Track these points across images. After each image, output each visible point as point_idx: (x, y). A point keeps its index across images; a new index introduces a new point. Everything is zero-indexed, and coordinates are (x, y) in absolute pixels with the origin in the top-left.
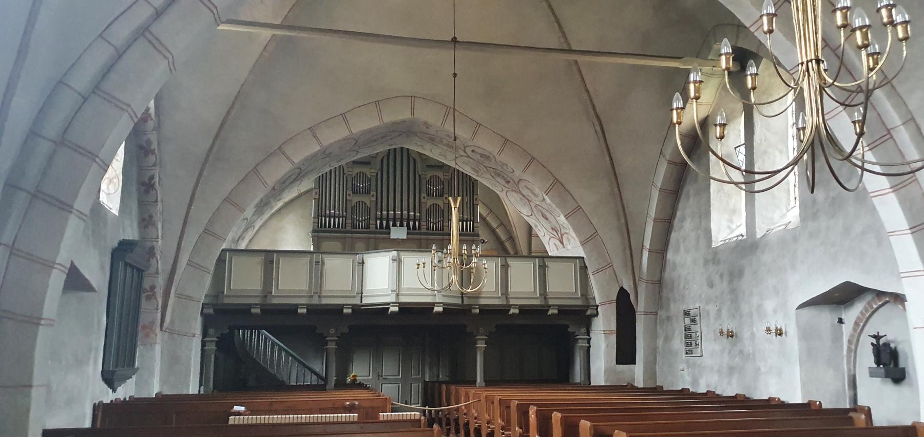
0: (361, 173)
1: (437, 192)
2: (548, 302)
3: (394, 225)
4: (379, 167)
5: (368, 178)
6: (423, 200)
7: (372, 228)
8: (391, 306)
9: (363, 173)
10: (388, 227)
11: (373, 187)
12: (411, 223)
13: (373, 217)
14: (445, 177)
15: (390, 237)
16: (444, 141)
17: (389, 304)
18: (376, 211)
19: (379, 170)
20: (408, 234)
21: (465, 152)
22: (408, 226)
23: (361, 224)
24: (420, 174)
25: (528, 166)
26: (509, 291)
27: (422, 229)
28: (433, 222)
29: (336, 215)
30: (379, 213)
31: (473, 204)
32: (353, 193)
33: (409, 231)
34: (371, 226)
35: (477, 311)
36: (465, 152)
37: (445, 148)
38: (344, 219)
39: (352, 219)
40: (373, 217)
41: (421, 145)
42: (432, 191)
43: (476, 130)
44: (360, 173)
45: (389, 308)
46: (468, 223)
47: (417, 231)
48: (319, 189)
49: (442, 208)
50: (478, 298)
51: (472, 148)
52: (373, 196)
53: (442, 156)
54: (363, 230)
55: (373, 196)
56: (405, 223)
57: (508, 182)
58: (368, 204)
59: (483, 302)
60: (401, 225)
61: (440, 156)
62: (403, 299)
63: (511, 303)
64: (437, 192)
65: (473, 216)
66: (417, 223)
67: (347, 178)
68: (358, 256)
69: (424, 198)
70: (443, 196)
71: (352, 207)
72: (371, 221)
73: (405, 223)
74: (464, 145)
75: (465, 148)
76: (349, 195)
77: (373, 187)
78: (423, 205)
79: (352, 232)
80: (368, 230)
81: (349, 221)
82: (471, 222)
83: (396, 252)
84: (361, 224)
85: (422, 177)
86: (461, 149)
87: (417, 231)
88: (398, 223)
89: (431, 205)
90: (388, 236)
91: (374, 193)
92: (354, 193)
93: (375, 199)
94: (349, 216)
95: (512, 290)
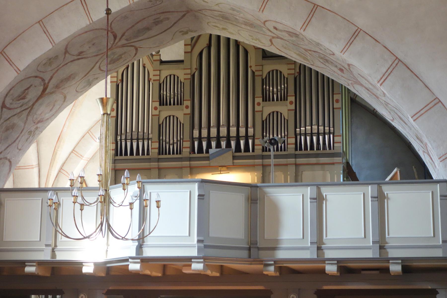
0: (172, 77)
2: (324, 254)
4: (195, 65)
6: (257, 108)
8: (131, 262)
9: (174, 76)
12: (242, 142)
17: (127, 260)
18: (193, 127)
19: (196, 69)
20: (234, 158)
24: (254, 71)
25: (350, 43)
26: (387, 236)
31: (333, 108)
35: (272, 268)
40: (187, 136)
45: (128, 265)
47: (251, 153)
49: (286, 118)
50: (274, 249)
52: (187, 107)
55: (187, 107)
56: (233, 143)
57: (341, 70)
58: (181, 119)
59: (281, 255)
62: (148, 253)
63: (390, 256)
66: (250, 141)
70: (287, 100)
73: (233, 143)
77: (187, 95)
78: (258, 116)
82: (331, 135)
85: (256, 73)
87: (243, 154)
88: (223, 144)
91: (188, 103)
95: (391, 236)
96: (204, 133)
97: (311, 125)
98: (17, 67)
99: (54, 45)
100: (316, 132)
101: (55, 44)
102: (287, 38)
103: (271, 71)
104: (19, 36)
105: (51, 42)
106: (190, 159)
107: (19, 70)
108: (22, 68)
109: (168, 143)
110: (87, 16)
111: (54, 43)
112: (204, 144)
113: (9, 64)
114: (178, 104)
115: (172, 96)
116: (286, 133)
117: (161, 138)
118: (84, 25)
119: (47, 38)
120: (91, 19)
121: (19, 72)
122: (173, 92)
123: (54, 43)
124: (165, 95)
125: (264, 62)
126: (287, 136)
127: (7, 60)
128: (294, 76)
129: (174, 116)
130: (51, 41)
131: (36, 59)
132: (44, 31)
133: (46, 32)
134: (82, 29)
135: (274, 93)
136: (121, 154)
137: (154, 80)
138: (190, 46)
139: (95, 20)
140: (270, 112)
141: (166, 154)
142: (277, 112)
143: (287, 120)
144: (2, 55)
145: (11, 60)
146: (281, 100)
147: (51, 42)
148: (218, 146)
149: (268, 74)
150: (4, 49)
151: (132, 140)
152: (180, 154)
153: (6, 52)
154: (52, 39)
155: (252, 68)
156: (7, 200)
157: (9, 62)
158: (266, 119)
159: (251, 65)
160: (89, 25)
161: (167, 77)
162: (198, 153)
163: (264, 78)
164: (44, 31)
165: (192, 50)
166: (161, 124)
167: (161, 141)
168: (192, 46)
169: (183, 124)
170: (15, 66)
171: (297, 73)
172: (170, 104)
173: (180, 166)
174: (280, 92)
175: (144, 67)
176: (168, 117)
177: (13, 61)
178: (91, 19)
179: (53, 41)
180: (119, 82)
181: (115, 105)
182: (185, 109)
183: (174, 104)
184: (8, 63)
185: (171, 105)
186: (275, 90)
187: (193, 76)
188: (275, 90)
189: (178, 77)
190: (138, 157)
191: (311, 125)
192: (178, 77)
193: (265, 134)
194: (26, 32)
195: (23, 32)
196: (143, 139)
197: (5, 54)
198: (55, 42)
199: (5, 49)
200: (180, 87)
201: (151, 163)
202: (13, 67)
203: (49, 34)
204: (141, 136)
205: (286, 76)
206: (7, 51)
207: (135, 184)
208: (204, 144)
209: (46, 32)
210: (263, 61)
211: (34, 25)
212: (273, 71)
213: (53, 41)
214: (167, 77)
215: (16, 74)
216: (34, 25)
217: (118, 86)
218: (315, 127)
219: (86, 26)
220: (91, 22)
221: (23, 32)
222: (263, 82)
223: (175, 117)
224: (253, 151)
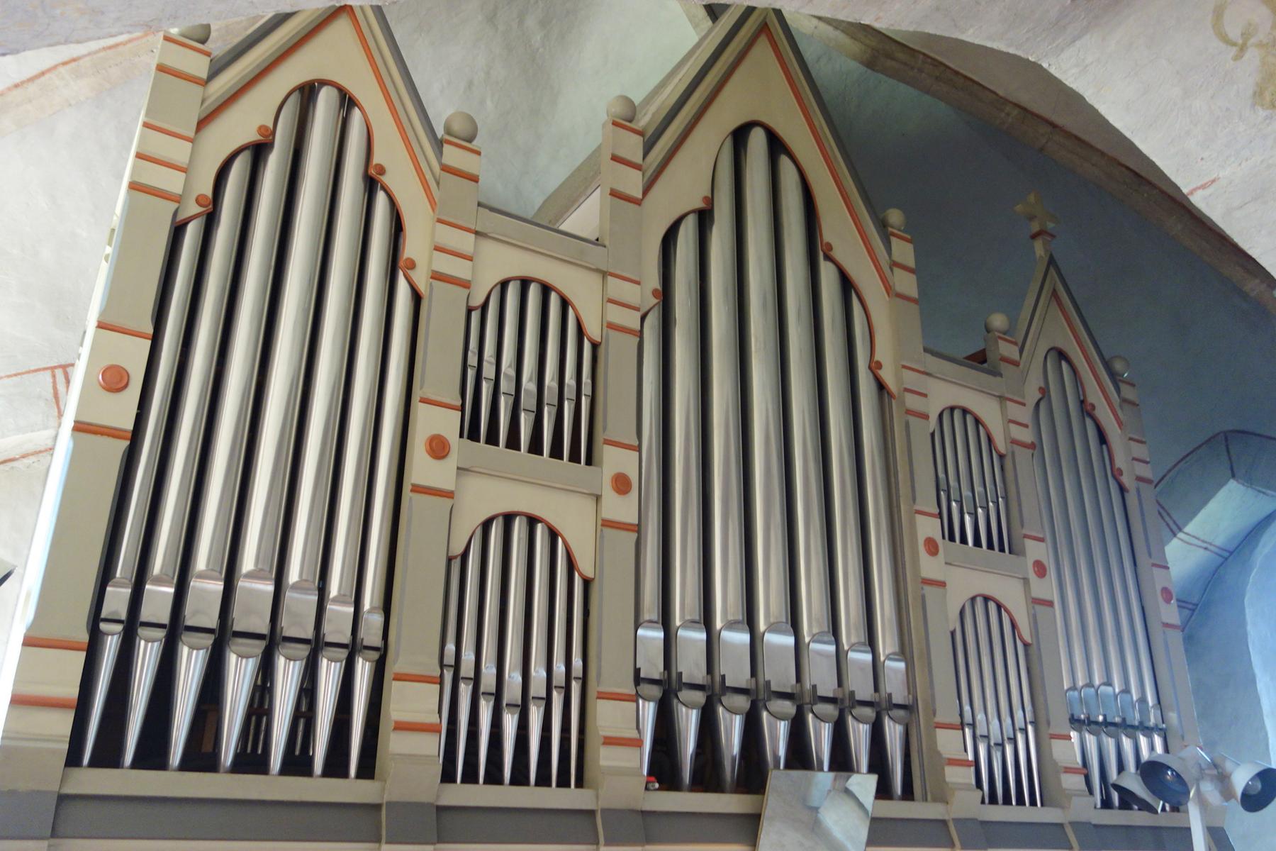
0: (533, 294)
9: (546, 290)
11: (616, 420)
23: (510, 723)
29: (288, 627)
38: (363, 671)
52: (621, 483)
84: (510, 723)
100: (165, 618)
115: (528, 401)
116: (577, 662)
117: (450, 647)
137: (437, 276)
141: (494, 777)
151: (175, 630)
161: (504, 285)
165: (646, 191)
166: (455, 557)
175: (371, 184)
176: (501, 519)
180: (194, 209)
181: (134, 355)
182: (609, 494)
183: (536, 447)
204: (298, 620)
214: (504, 285)
217: (178, 231)
223: (539, 527)
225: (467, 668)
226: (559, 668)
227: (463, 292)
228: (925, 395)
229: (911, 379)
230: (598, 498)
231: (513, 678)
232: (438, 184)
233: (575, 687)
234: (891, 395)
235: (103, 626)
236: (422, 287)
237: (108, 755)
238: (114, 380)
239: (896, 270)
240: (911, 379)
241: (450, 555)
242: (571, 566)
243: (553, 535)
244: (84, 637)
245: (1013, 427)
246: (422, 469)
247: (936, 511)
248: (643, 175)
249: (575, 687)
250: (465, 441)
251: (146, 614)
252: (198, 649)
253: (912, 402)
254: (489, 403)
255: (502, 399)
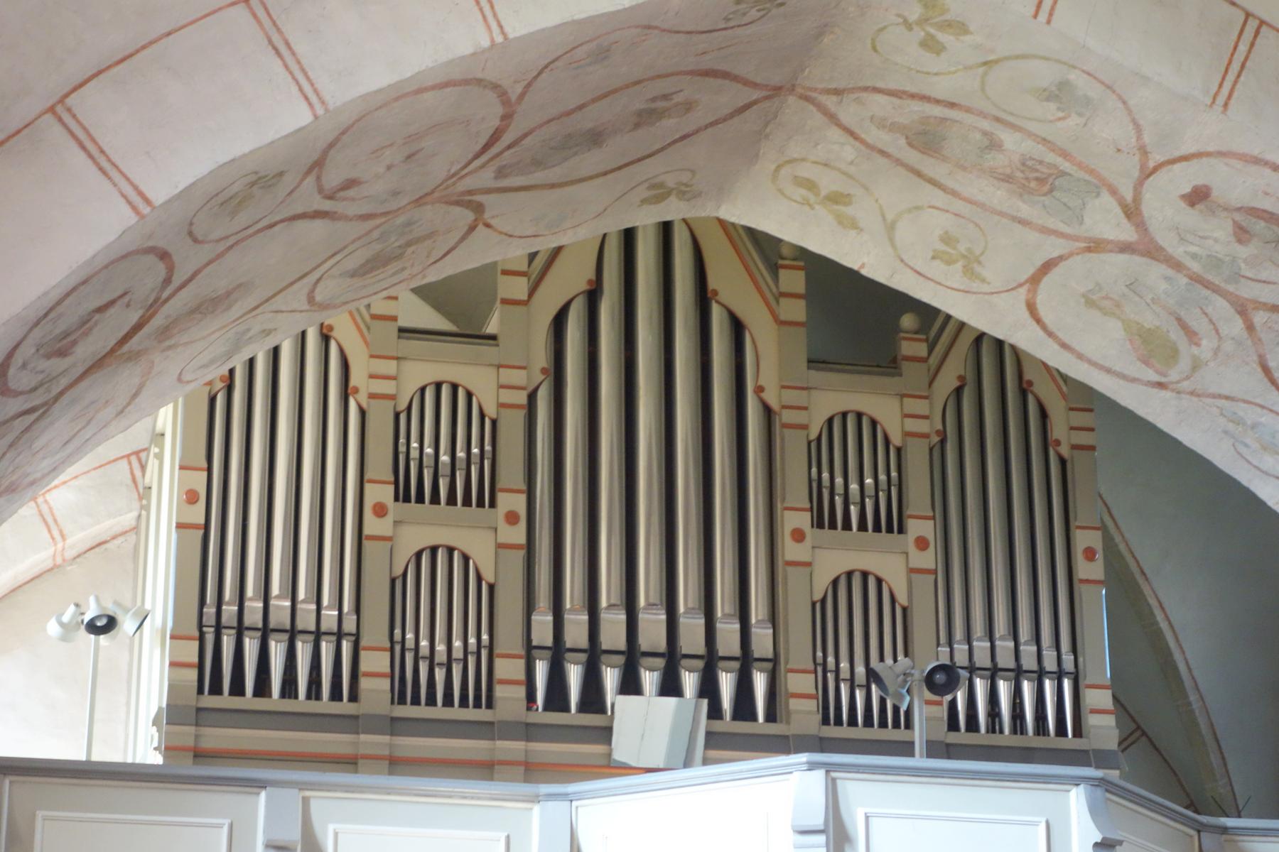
0: (445, 392)
1: (869, 503)
3: (630, 685)
4: (541, 357)
5: (482, 416)
6: (790, 550)
7: (509, 697)
9: (455, 387)
10: (593, 699)
11: (511, 471)
13: (509, 636)
14: (912, 425)
15: (609, 755)
16: (1009, 139)
21: (1132, 212)
22: (708, 689)
23: (440, 675)
24: (774, 403)
27: (794, 717)
28: (852, 680)
29: (300, 625)
30: (543, 622)
32: (403, 495)
33: (718, 726)
34: (499, 691)
36: (1132, 212)
37: (998, 195)
38: (346, 646)
39: (392, 650)
40: (509, 636)
41: (836, 199)
42: (839, 500)
43: (1243, 48)
44: (438, 386)
46: (1048, 685)
48: (209, 470)
51: (1184, 178)
53: (949, 262)
54: (456, 713)
55: (512, 518)
56: (689, 681)
58: (483, 558)
60: (670, 687)
61: (937, 269)
64: (869, 503)
65: (1074, 650)
66: (760, 682)
67: (363, 413)
68: (536, 809)
69: (798, 536)
71: (393, 581)
72: (498, 663)
73: (689, 681)
74: (1144, 151)
75: (1139, 184)
76: (380, 511)
77: (511, 471)
79: (395, 726)
80: (483, 714)
81: (375, 661)
82: (1067, 684)
83: (819, 775)
84: (440, 675)
85: (788, 416)
86: (1113, 192)
88: (649, 679)
89: (835, 583)
90: (599, 749)
91: (517, 503)
92: (407, 499)
93: (522, 539)
94: (375, 632)
96: (576, 633)
97: (969, 639)
98: (136, 188)
99: (320, 111)
101: (327, 110)
102: (1193, 249)
103: (837, 414)
104: (144, 47)
105: (306, 98)
106: (530, 732)
107: (147, 201)
108: (160, 193)
109: (423, 658)
110: (481, 10)
111: (323, 103)
112: (574, 675)
113: (94, 169)
114: (467, 502)
115: (445, 470)
117: (398, 632)
118: (465, 48)
119: (290, 79)
120: (501, 27)
121: (146, 210)
122: (449, 451)
123: (323, 103)
124: (414, 459)
125: (816, 377)
126: (834, 674)
127: (83, 148)
128: (930, 442)
129: (451, 550)
130: (309, 93)
131: (233, 160)
132: (270, 42)
133: (281, 48)
134: (450, 63)
135: (851, 500)
136: (216, 689)
138: (524, 280)
139: (517, 34)
140: (840, 573)
142: (865, 575)
143: (905, 610)
144: (60, 120)
145: (105, 148)
146: (877, 528)
147: (306, 98)
148: (630, 685)
149: (826, 423)
150: (67, 95)
152: (490, 705)
153: (76, 110)
154: (312, 85)
155: (764, 395)
156: (44, 819)
157: (91, 156)
158: (823, 601)
159: (761, 382)
160: (484, 51)
161: (423, 390)
162: (548, 706)
163: (814, 440)
164: (270, 42)
165: (531, 293)
166: (398, 577)
167: (398, 648)
168: (531, 281)
169: (491, 588)
170: (128, 179)
171: (938, 432)
172: (435, 499)
173: (484, 757)
174: (874, 498)
176: (428, 551)
177: (112, 157)
178: (501, 27)
179: (316, 91)
183: (452, 500)
184: (89, 162)
185: (439, 503)
186: (854, 487)
187: (532, 397)
188: (854, 487)
189: (469, 395)
190: (288, 705)
191: (969, 639)
192: (469, 395)
193: (819, 654)
194: (178, 33)
195: (169, 34)
196: (293, 634)
197: (74, 116)
198: (327, 98)
199: (73, 96)
200: (479, 437)
201: (363, 737)
202: (115, 185)
203: (299, 62)
205: (896, 440)
206: (83, 103)
207: (791, 773)
208: (574, 675)
209: (281, 48)
210: (812, 372)
211: (220, 9)
212: (844, 415)
213: (316, 91)
214: (423, 390)
215: (133, 219)
216: (220, 9)
218: (981, 646)
219: (474, 54)
220: (499, 39)
221: (169, 34)
222: (817, 450)
223: (456, 553)
224: (771, 717)
225: (410, 643)
226: (472, 640)
227: (391, 403)
228: (805, 408)
229: (792, 397)
230: (496, 530)
231: (441, 647)
232: (368, 328)
233: (484, 653)
234: (775, 413)
235: (205, 629)
236: (364, 405)
237: (216, 689)
238: (192, 497)
239: (783, 301)
240: (792, 397)
241: (393, 575)
242: (479, 579)
243: (466, 559)
244: (197, 634)
245: (908, 421)
246: (373, 525)
247: (808, 506)
248: (529, 280)
249: (484, 653)
250: (400, 504)
251: (225, 619)
252: (254, 639)
253: (788, 416)
254: (417, 475)
255: (426, 471)
